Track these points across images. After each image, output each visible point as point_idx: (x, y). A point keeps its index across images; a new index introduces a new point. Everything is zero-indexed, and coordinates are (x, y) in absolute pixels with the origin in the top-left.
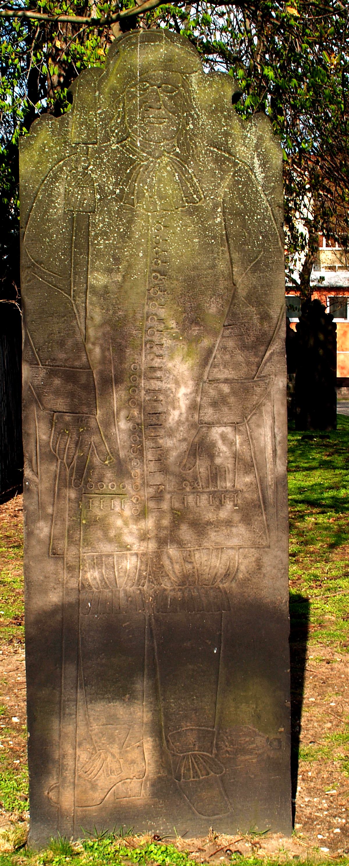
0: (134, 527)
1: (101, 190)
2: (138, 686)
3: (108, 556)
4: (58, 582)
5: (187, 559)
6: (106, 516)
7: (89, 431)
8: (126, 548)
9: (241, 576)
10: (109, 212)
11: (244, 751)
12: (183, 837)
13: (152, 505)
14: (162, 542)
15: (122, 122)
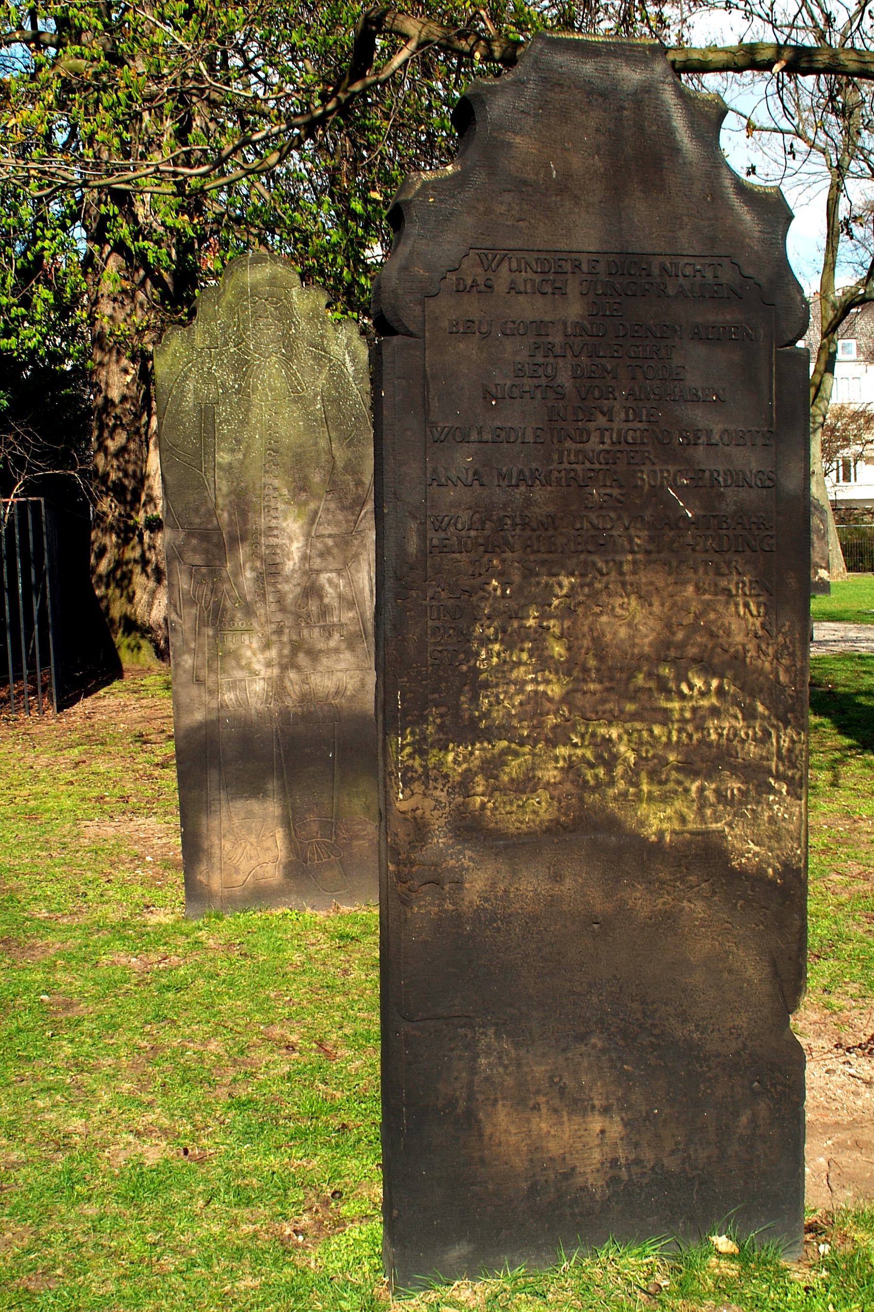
0: (260, 657)
1: (223, 385)
2: (270, 786)
3: (241, 681)
4: (201, 703)
5: (305, 681)
6: (238, 649)
7: (221, 580)
8: (256, 674)
9: (348, 693)
10: (230, 402)
11: (357, 837)
12: (312, 908)
13: (274, 638)
14: (284, 668)
15: (238, 330)
